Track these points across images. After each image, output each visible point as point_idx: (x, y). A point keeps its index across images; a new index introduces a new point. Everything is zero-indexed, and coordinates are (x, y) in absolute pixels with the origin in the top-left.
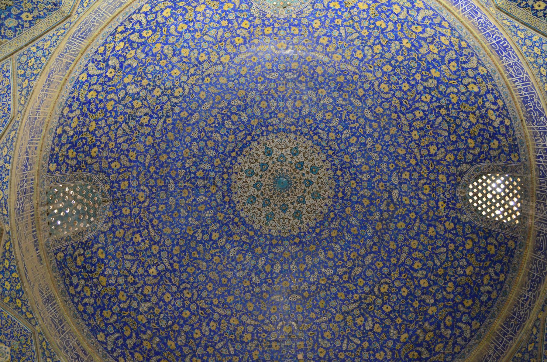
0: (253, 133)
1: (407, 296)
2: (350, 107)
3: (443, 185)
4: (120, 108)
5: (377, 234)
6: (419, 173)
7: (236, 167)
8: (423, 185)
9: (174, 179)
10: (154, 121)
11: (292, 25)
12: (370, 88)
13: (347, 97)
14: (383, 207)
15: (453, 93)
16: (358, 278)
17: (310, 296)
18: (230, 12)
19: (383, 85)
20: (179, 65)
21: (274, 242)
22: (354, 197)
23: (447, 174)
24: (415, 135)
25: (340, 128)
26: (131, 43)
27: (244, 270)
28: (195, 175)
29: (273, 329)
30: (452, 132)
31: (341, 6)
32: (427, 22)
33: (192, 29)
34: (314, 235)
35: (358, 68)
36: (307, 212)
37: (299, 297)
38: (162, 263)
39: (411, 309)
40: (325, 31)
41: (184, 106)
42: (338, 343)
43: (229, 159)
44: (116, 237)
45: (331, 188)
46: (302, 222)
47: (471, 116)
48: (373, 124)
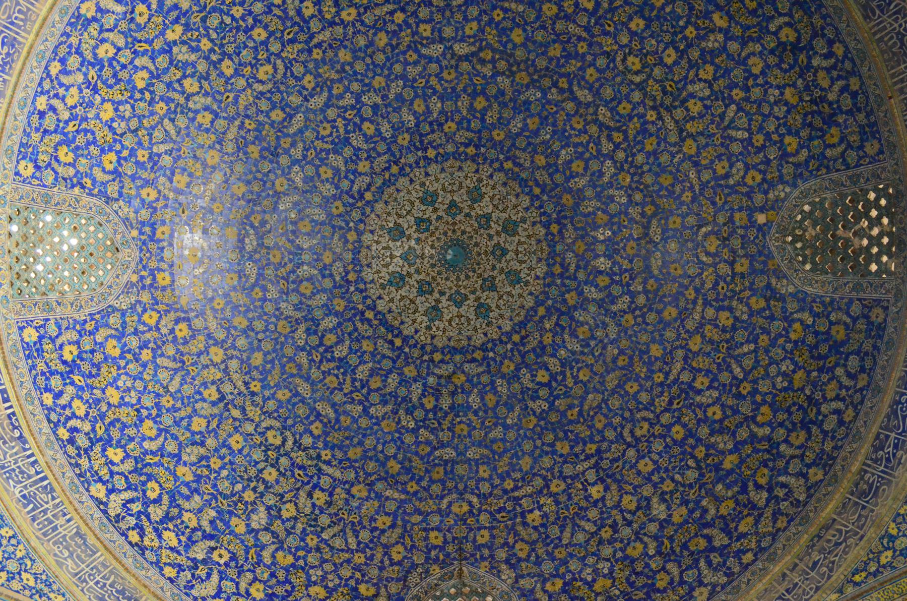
0: (360, 307)
1: (644, 18)
4: (292, 541)
7: (422, 337)
9: (435, 449)
10: (325, 482)
11: (152, 238)
12: (269, 99)
13: (289, 140)
14: (487, 70)
17: (653, 203)
19: (261, 76)
20: (223, 435)
21: (557, 269)
25: (348, 152)
26: (167, 518)
27: (605, 325)
29: (711, 269)
31: (110, 150)
33: (154, 412)
34: (545, 198)
37: (654, 222)
38: (583, 473)
39: (668, 10)
40: (162, 180)
41: (300, 428)
42: (736, 148)
43: (407, 350)
44: (529, 556)
45: (460, 168)
46: (524, 221)
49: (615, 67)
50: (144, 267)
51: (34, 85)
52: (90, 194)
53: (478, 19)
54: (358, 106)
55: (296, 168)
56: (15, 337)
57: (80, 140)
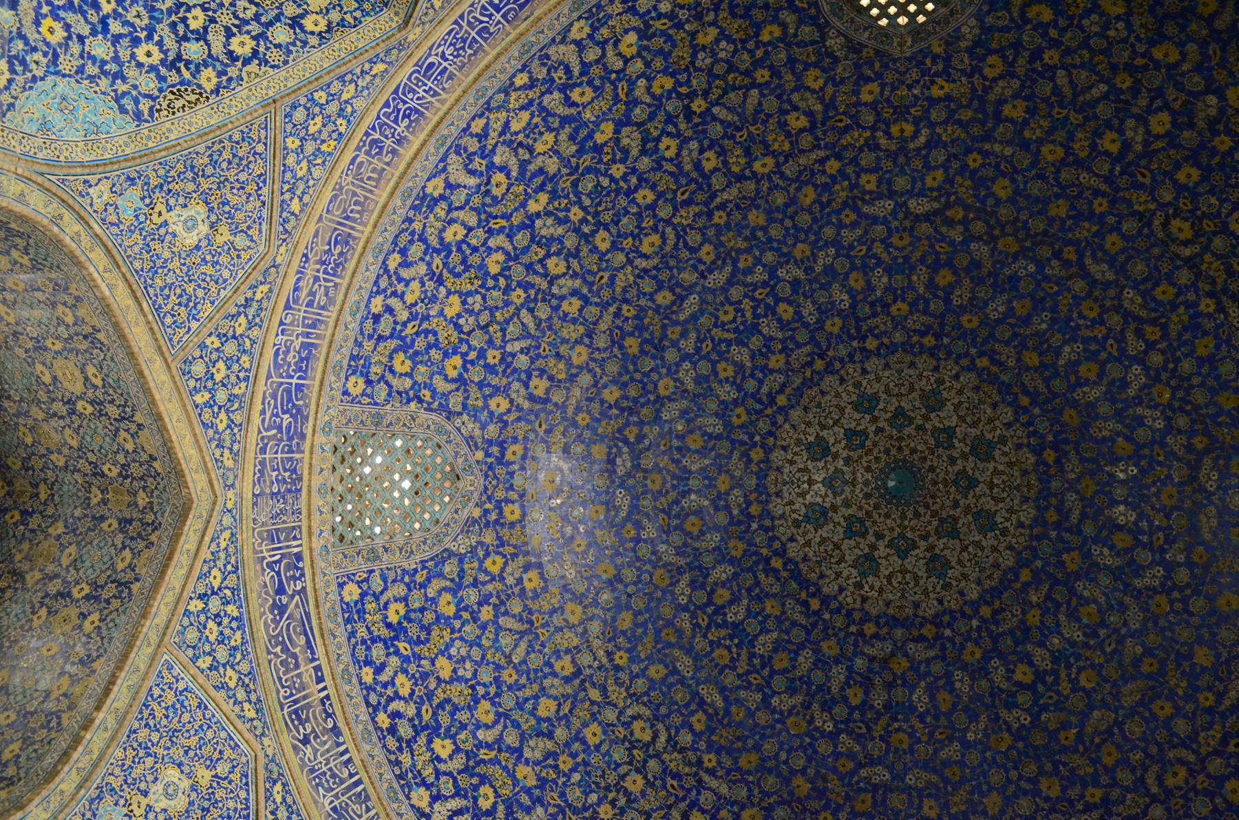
0: (765, 551)
2: (703, 320)
3: (888, 89)
5: (1029, 249)
6: (861, 150)
7: (848, 598)
8: (890, 137)
9: (860, 766)
10: (706, 799)
11: (500, 460)
12: (654, 278)
14: (956, 235)
15: (648, 89)
16: (1154, 299)
17: (1207, 433)
18: (462, 600)
19: (645, 248)
20: (576, 723)
21: (1052, 516)
22: (932, 306)
23: (857, 83)
24: (764, 165)
25: (756, 343)
27: (1123, 608)
28: (856, 708)
30: (747, 81)
31: (455, 353)
32: (479, 164)
33: (492, 690)
34: (1037, 411)
35: (604, 306)
36: (974, 425)
37: (1207, 461)
40: (516, 385)
41: (677, 720)
43: (827, 616)
46: (1003, 440)
47: (701, 39)
48: (741, 265)
49: (1152, 233)
50: (489, 499)
51: (369, 285)
52: (429, 409)
53: (945, 167)
54: (771, 282)
55: (687, 365)
56: (334, 597)
57: (420, 344)
